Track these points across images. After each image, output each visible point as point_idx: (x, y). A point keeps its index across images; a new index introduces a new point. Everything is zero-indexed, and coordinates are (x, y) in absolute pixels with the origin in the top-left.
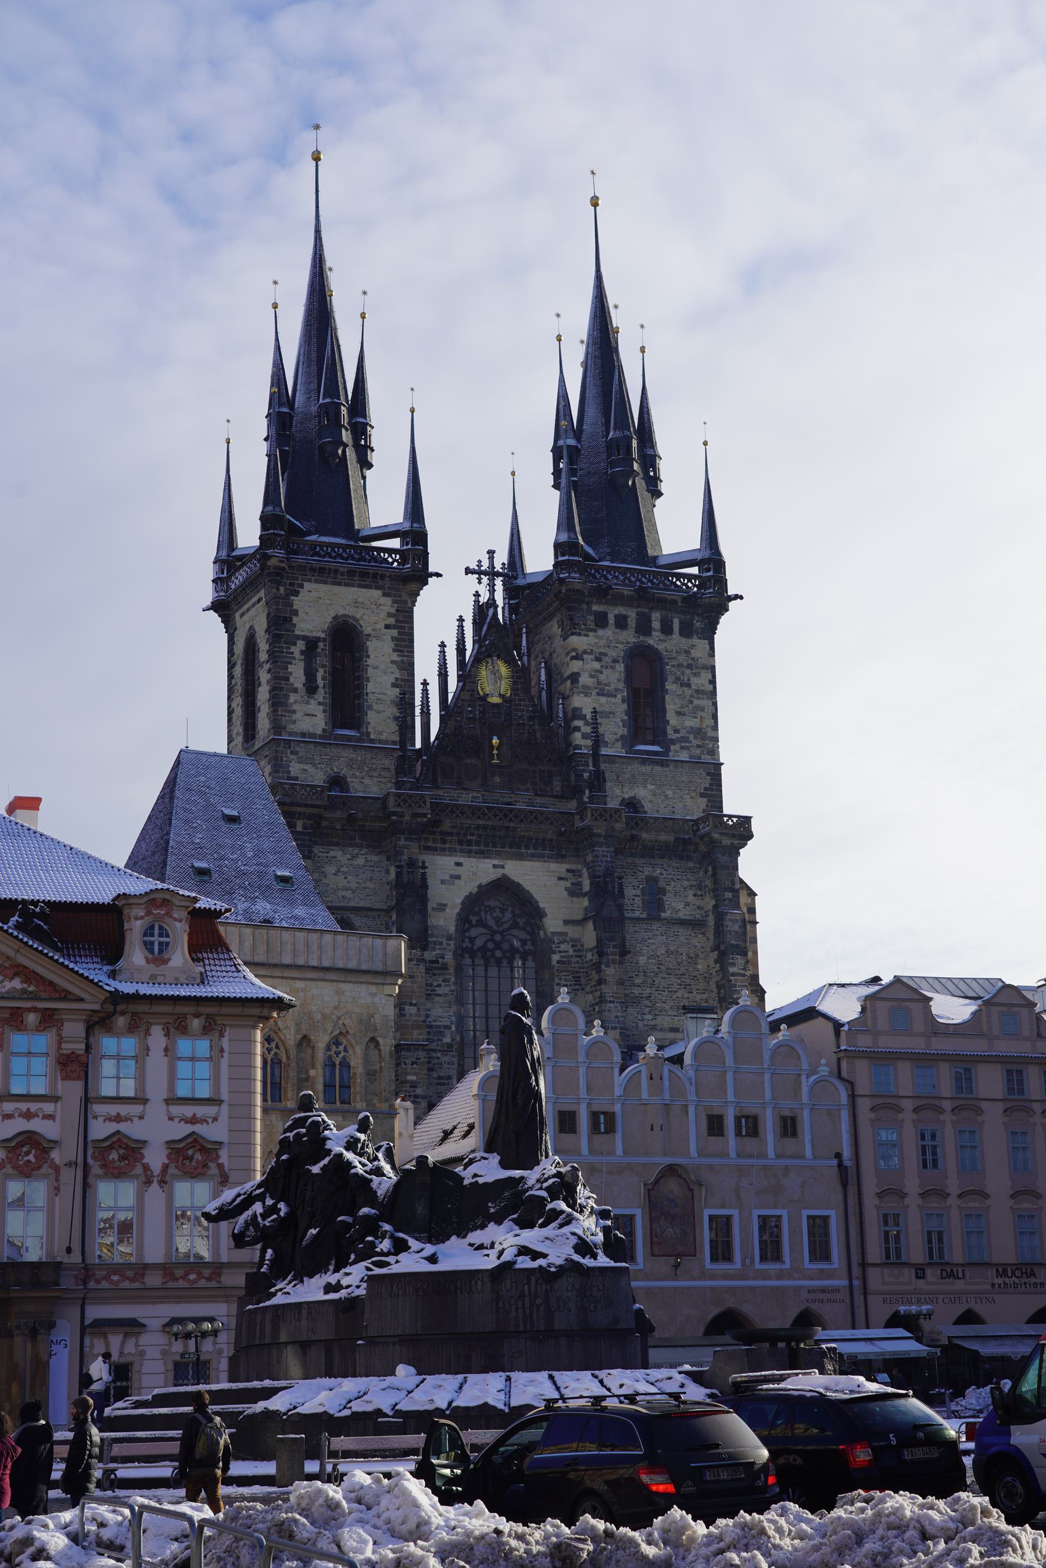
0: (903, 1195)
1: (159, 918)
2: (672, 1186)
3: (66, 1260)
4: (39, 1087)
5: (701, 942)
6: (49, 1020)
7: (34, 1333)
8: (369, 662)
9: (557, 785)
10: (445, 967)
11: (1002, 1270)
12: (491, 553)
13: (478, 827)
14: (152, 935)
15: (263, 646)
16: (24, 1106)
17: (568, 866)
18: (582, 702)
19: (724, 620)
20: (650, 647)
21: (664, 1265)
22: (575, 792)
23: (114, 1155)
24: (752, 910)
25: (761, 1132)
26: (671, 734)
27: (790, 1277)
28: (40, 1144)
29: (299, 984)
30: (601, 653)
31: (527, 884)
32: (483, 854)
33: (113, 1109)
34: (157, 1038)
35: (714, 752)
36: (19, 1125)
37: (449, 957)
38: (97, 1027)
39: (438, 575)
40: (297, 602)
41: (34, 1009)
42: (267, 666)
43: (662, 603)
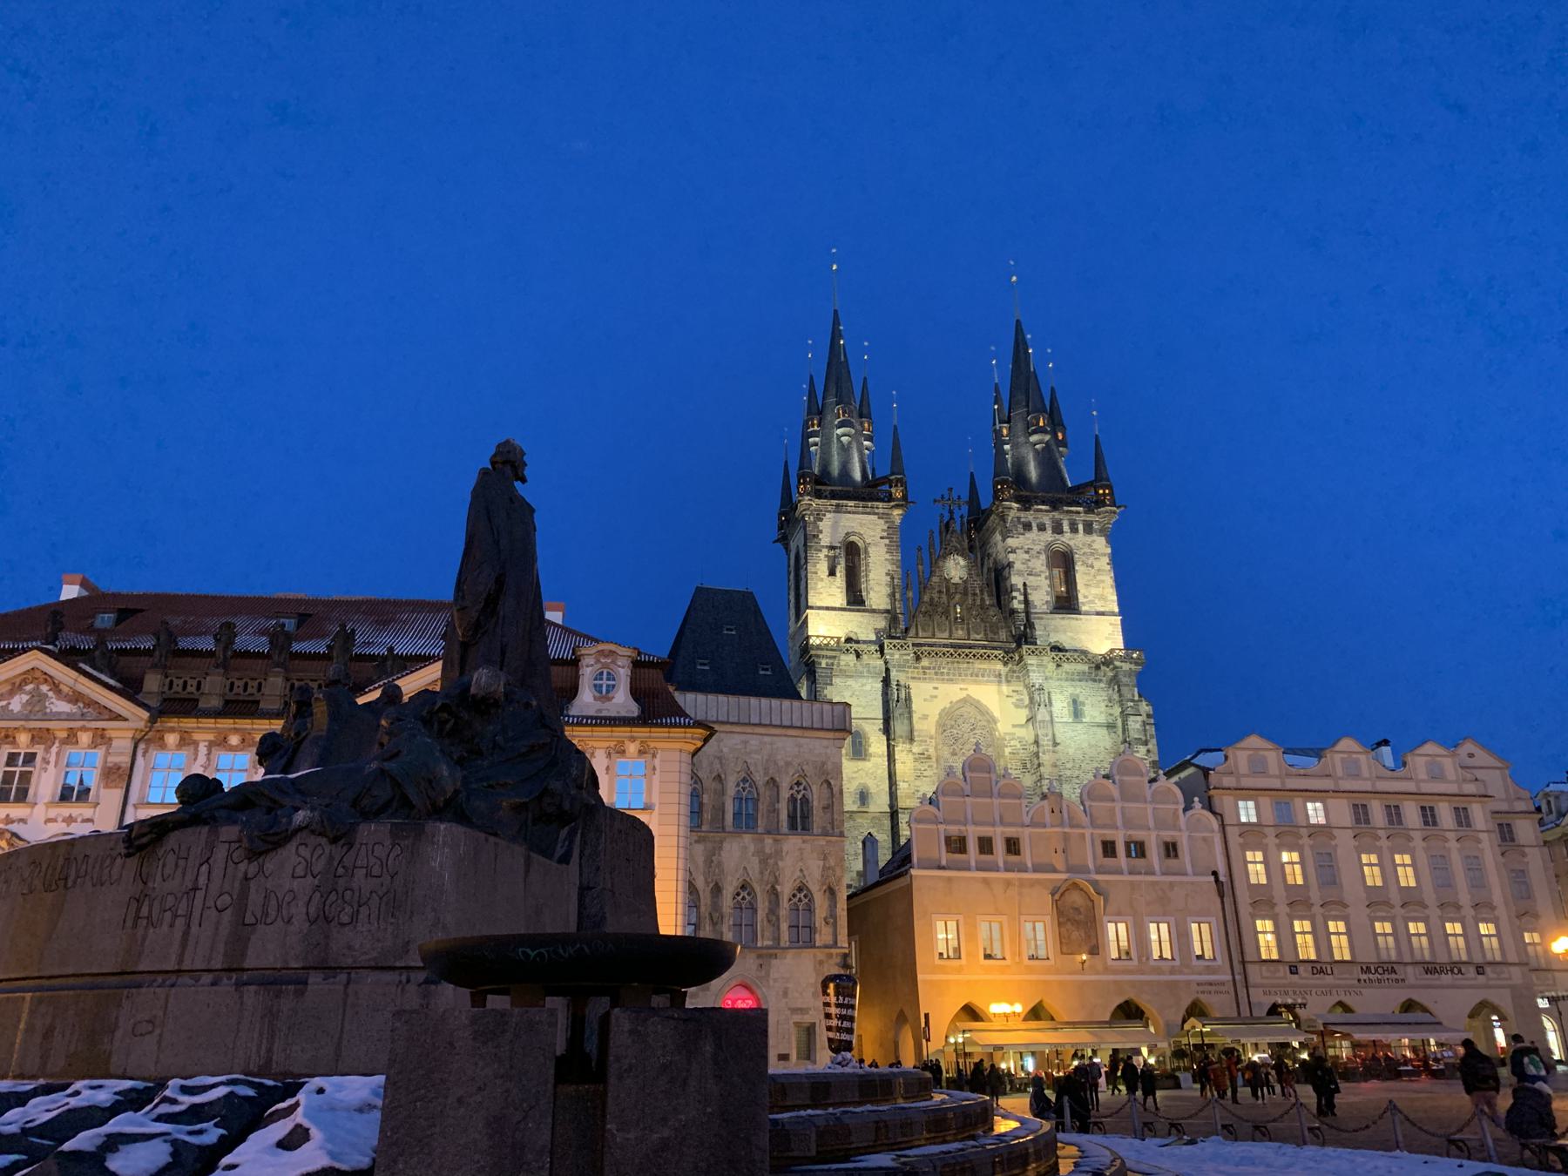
1: (605, 666)
10: (929, 758)
18: (1016, 580)
25: (1148, 853)
27: (1181, 973)
29: (767, 739)
37: (932, 751)
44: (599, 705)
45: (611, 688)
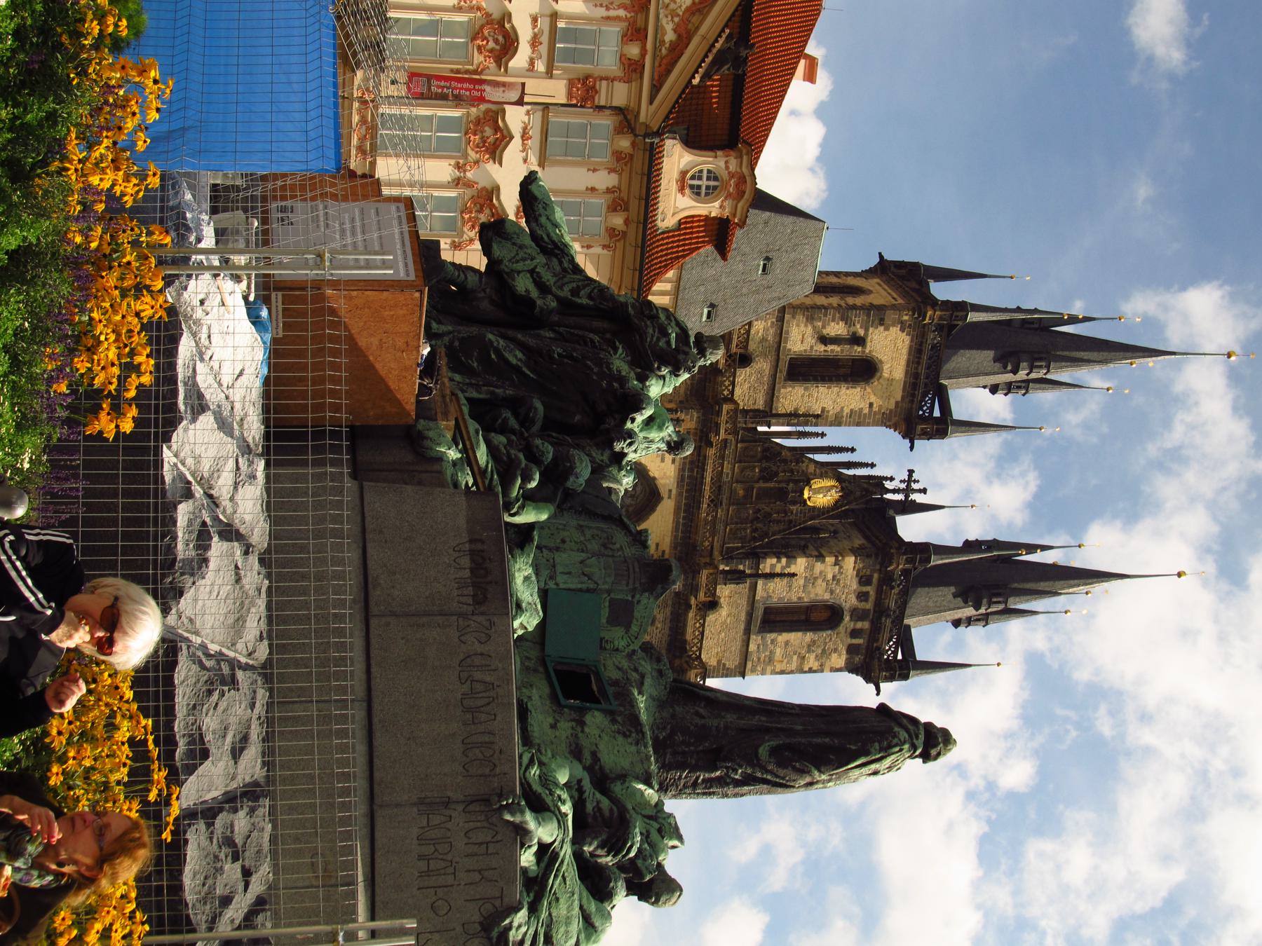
1: (727, 185)
6: (633, 69)
8: (844, 390)
12: (924, 491)
13: (703, 477)
14: (708, 179)
15: (859, 301)
16: (545, 39)
17: (667, 552)
19: (860, 680)
20: (841, 619)
23: (488, 131)
26: (770, 636)
28: (506, 54)
30: (838, 581)
32: (681, 480)
33: (535, 132)
34: (604, 180)
35: (753, 671)
36: (524, 32)
38: (621, 117)
39: (912, 448)
40: (895, 331)
41: (644, 52)
42: (842, 303)
44: (676, 175)
45: (696, 191)
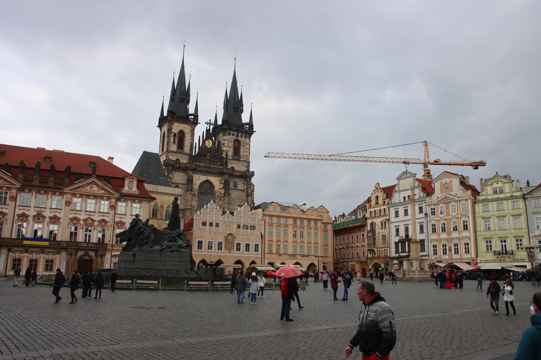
0: (273, 241)
2: (230, 237)
3: (108, 243)
4: (106, 211)
5: (244, 194)
6: (108, 198)
7: (102, 256)
9: (219, 163)
11: (290, 255)
16: (103, 214)
18: (224, 148)
21: (227, 251)
22: (222, 165)
24: (253, 189)
31: (212, 181)
33: (120, 216)
36: (102, 218)
37: (196, 194)
40: (173, 126)
43: (241, 132)
